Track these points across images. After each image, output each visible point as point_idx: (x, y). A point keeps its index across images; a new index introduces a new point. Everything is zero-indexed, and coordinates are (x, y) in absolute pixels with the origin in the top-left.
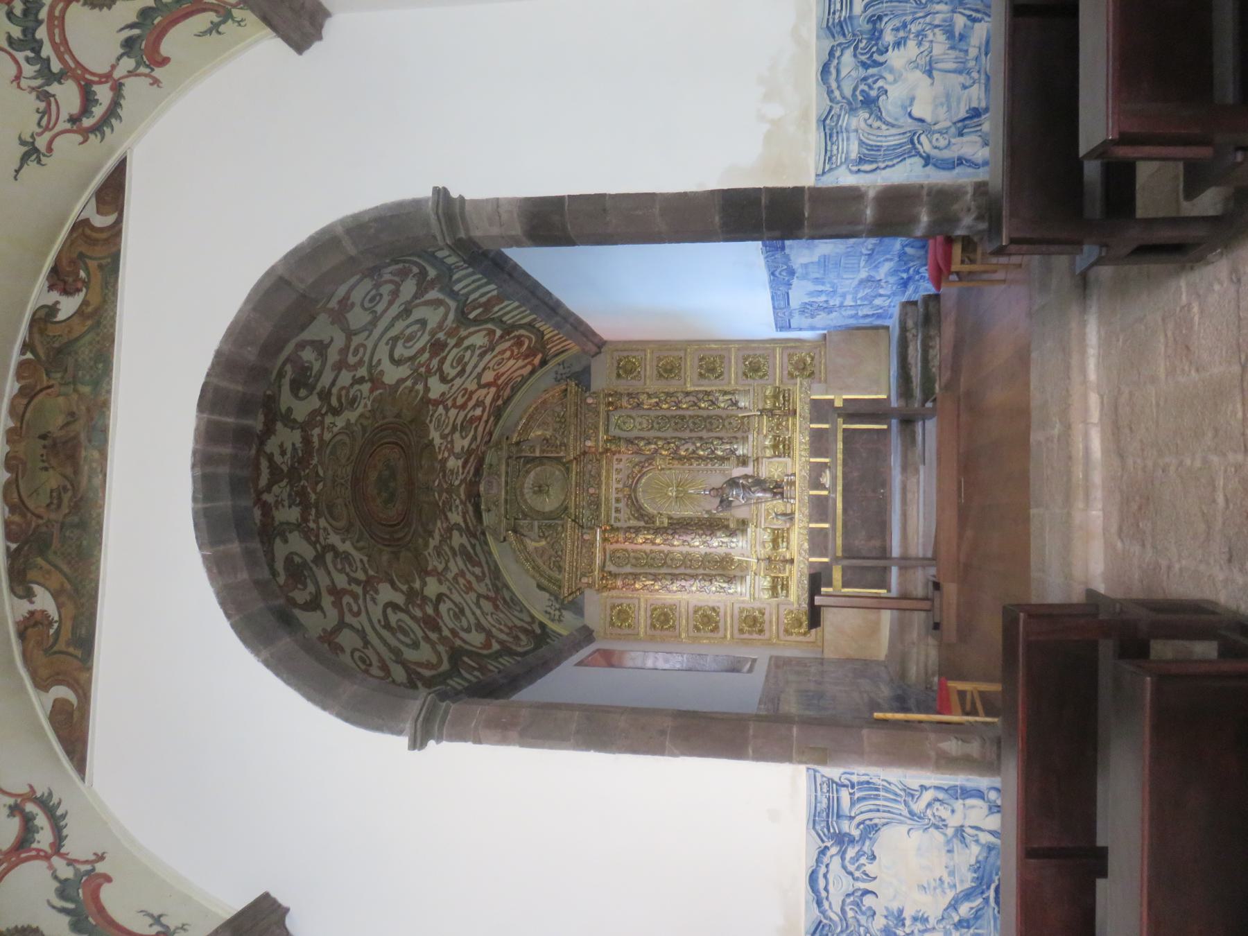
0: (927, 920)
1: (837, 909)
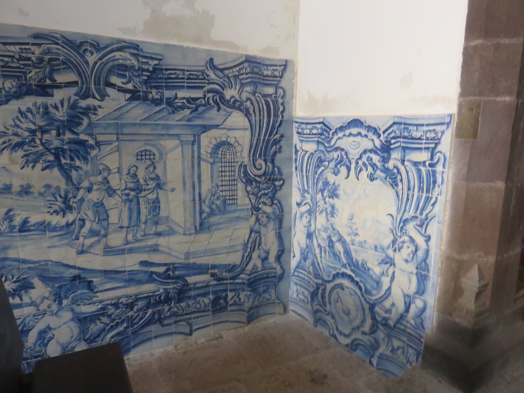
0: (332, 216)
1: (340, 144)
